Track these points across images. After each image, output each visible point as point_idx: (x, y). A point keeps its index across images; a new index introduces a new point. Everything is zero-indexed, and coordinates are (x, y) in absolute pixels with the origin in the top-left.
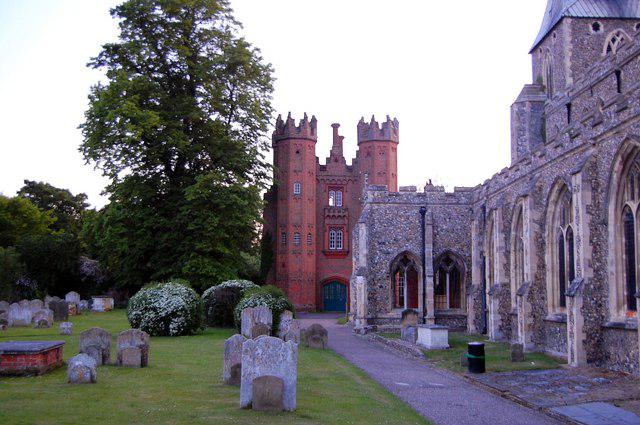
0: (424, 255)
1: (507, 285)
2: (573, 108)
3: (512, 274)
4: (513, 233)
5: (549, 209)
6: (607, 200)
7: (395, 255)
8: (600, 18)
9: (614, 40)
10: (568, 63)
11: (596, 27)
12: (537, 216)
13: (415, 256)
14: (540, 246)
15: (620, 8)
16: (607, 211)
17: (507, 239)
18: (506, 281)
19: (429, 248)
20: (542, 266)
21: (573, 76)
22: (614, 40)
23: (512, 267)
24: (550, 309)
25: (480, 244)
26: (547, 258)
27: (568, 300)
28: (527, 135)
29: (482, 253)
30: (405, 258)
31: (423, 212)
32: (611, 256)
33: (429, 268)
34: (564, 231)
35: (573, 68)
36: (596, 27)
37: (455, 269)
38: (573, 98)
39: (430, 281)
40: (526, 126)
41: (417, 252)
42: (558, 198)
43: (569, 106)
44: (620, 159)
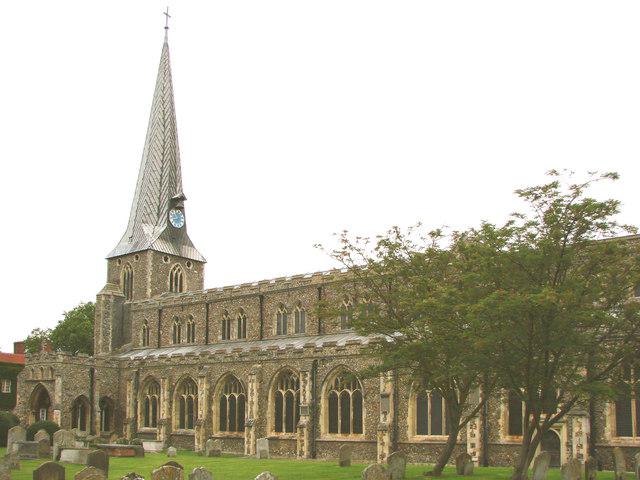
0: (92, 398)
1: (170, 420)
3: (173, 414)
4: (175, 392)
9: (174, 269)
10: (150, 280)
11: (166, 260)
13: (87, 400)
14: (210, 401)
17: (171, 395)
19: (97, 396)
20: (210, 412)
25: (135, 394)
26: (213, 408)
28: (111, 318)
29: (136, 400)
30: (80, 399)
31: (92, 371)
32: (269, 410)
33: (97, 407)
34: (227, 397)
36: (166, 260)
38: (164, 307)
40: (111, 312)
41: (88, 396)
43: (160, 311)
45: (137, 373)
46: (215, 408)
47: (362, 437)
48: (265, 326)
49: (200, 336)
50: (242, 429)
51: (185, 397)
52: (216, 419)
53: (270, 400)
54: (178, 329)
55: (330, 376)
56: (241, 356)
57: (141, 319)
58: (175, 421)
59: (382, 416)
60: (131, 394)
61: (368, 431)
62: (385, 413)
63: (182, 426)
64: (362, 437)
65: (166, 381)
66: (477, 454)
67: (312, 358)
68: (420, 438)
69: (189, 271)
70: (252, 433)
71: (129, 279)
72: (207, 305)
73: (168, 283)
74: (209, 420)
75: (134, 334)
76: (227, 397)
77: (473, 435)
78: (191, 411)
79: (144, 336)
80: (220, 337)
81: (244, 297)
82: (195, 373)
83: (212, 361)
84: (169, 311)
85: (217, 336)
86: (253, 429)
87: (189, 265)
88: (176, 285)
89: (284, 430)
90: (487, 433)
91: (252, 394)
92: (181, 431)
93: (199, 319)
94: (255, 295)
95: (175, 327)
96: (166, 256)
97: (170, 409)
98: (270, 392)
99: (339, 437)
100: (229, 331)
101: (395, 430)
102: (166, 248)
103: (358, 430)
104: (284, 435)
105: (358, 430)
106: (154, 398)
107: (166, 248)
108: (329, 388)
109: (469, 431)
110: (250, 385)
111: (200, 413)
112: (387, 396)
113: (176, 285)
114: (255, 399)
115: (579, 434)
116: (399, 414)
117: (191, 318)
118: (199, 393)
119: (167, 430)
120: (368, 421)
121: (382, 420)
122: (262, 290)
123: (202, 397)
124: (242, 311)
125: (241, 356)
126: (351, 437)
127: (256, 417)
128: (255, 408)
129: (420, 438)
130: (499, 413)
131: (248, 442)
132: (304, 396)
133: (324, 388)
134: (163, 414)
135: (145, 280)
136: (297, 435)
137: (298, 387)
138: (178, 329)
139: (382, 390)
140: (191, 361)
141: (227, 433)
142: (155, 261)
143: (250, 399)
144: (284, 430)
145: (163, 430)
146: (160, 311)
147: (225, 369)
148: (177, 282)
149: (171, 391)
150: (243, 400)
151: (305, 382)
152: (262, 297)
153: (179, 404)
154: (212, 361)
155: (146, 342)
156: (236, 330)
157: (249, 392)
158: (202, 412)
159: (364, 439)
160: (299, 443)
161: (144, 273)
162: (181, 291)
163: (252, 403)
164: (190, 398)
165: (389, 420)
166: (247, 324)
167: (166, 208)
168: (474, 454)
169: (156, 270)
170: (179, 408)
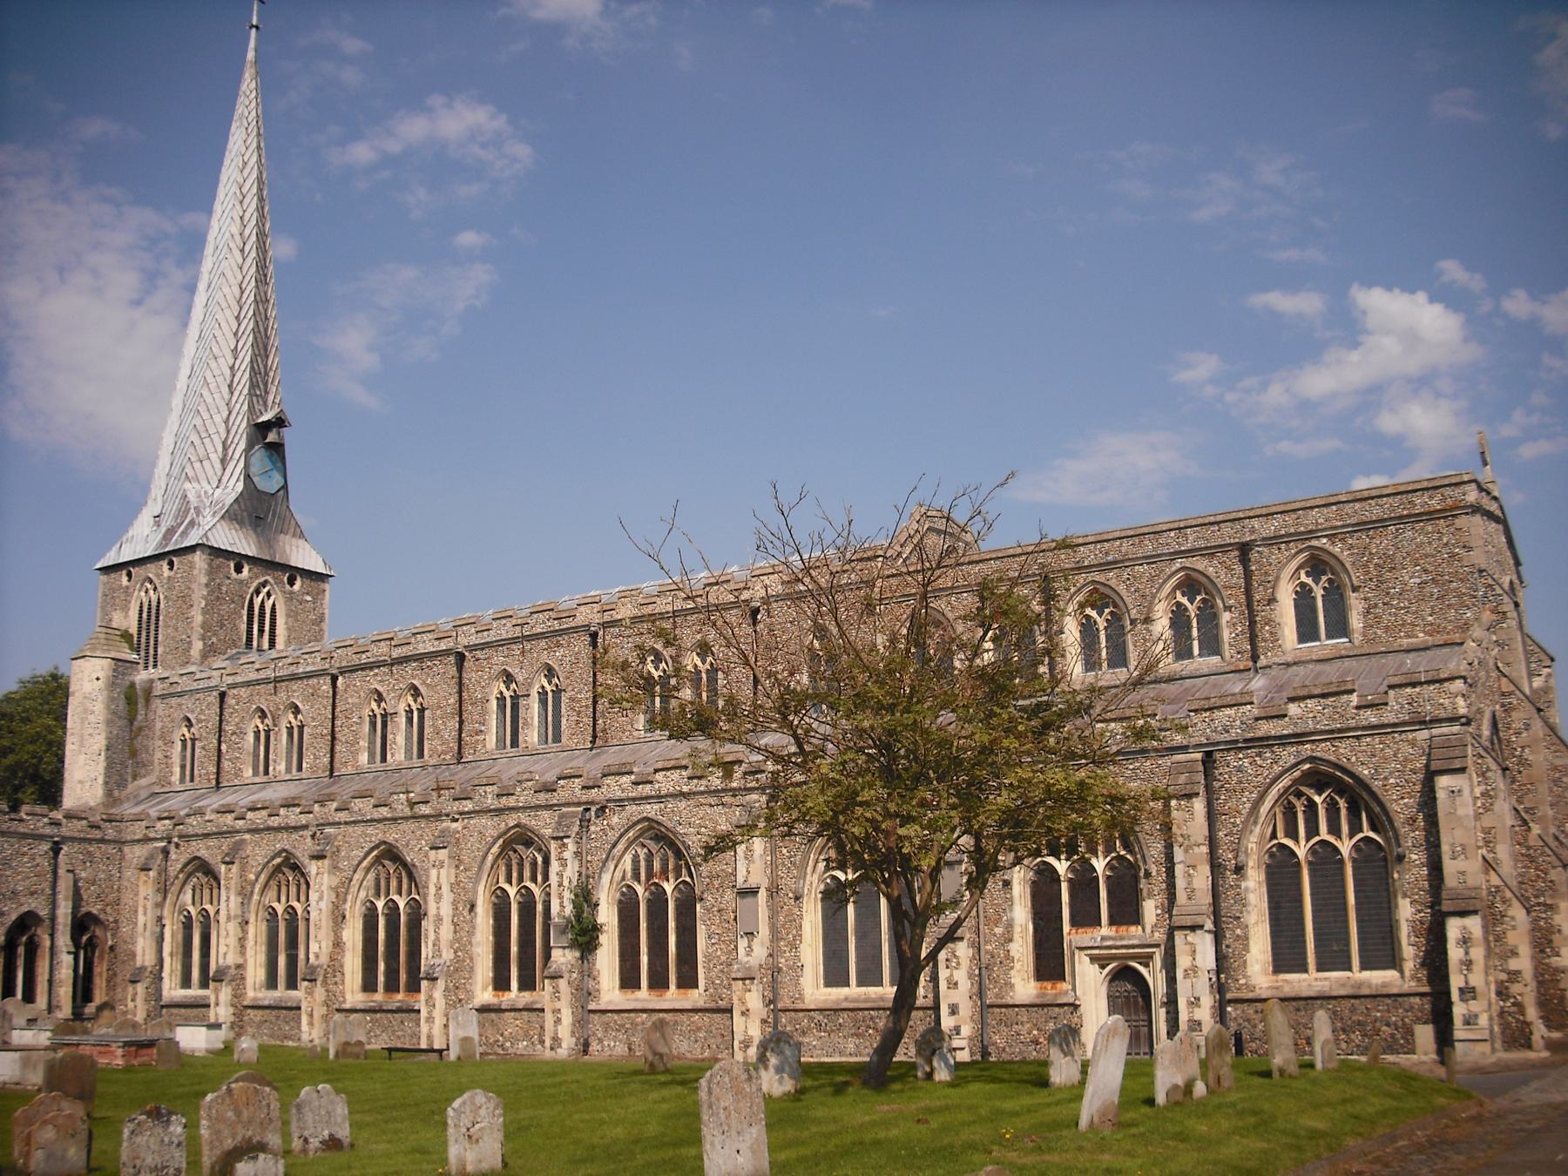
0: (53, 918)
2: (230, 701)
3: (250, 952)
4: (256, 897)
5: (356, 876)
6: (477, 882)
7: (14, 917)
8: (246, 556)
10: (199, 619)
11: (239, 569)
12: (335, 881)
14: (339, 918)
15: (269, 543)
16: (476, 892)
18: (241, 961)
20: (338, 944)
21: (203, 638)
22: (258, 592)
23: (250, 943)
24: (349, 997)
27: (424, 984)
29: (160, 919)
30: (27, 922)
33: (64, 940)
34: (380, 904)
35: (206, 626)
37: (90, 940)
39: (66, 960)
41: (43, 913)
42: (372, 865)
43: (223, 695)
44: (501, 841)
45: (166, 852)
46: (353, 934)
47: (696, 997)
48: (467, 727)
49: (316, 757)
50: (414, 987)
51: (280, 908)
52: (353, 963)
53: (480, 909)
54: (265, 738)
55: (620, 846)
56: (412, 804)
57: (178, 715)
58: (256, 972)
59: (743, 943)
60: (149, 905)
61: (710, 982)
62: (750, 934)
63: (271, 982)
64: (696, 997)
65: (235, 868)
66: (966, 1031)
67: (579, 804)
68: (837, 994)
69: (290, 597)
70: (438, 995)
71: (150, 618)
72: (334, 679)
73: (244, 627)
74: (335, 967)
75: (159, 755)
76: (380, 904)
77: (953, 985)
78: (292, 943)
79: (183, 758)
80: (364, 758)
81: (419, 658)
82: (302, 847)
83: (343, 816)
84: (244, 692)
85: (355, 754)
86: (441, 984)
87: (291, 582)
88: (261, 631)
89: (514, 984)
90: (985, 974)
91: (438, 897)
92: (269, 997)
93: (314, 714)
94: (447, 652)
95: (257, 733)
96: (240, 560)
97: (242, 941)
98: (481, 889)
99: (644, 996)
100: (384, 737)
101: (775, 976)
102: (243, 543)
103: (688, 980)
104: (514, 995)
105: (688, 980)
106: (205, 914)
107: (243, 543)
108: (618, 875)
109: (943, 974)
110: (434, 872)
111: (314, 947)
112: (753, 892)
113: (261, 631)
114: (446, 910)
115: (1192, 971)
116: (784, 934)
117: (296, 711)
118: (313, 896)
119: (235, 996)
120: (708, 956)
121: (741, 951)
122: (463, 641)
123: (319, 905)
124: (416, 693)
125: (412, 804)
126: (673, 997)
127: (447, 955)
128: (446, 932)
129: (837, 994)
130: (1010, 926)
131: (430, 1019)
132: (561, 897)
133: (606, 878)
134: (224, 951)
135: (188, 620)
136: (543, 995)
137: (546, 878)
138: (265, 738)
139: (740, 880)
140: (293, 816)
141: (379, 997)
142: (211, 572)
143: (432, 908)
144: (514, 984)
145: (225, 993)
146: (223, 695)
147: (376, 834)
148: (260, 623)
149: (245, 895)
150: (417, 914)
151: (563, 863)
152: (461, 658)
153: (263, 926)
154: (343, 816)
155: (188, 772)
156: (401, 739)
157: (432, 890)
158: (318, 947)
159: (701, 1004)
160: (549, 1018)
161: (185, 600)
162: (272, 644)
163: (439, 919)
164: (291, 911)
165: (760, 951)
166: (428, 723)
167: (242, 446)
168: (957, 1030)
169: (215, 596)
170: (263, 938)
